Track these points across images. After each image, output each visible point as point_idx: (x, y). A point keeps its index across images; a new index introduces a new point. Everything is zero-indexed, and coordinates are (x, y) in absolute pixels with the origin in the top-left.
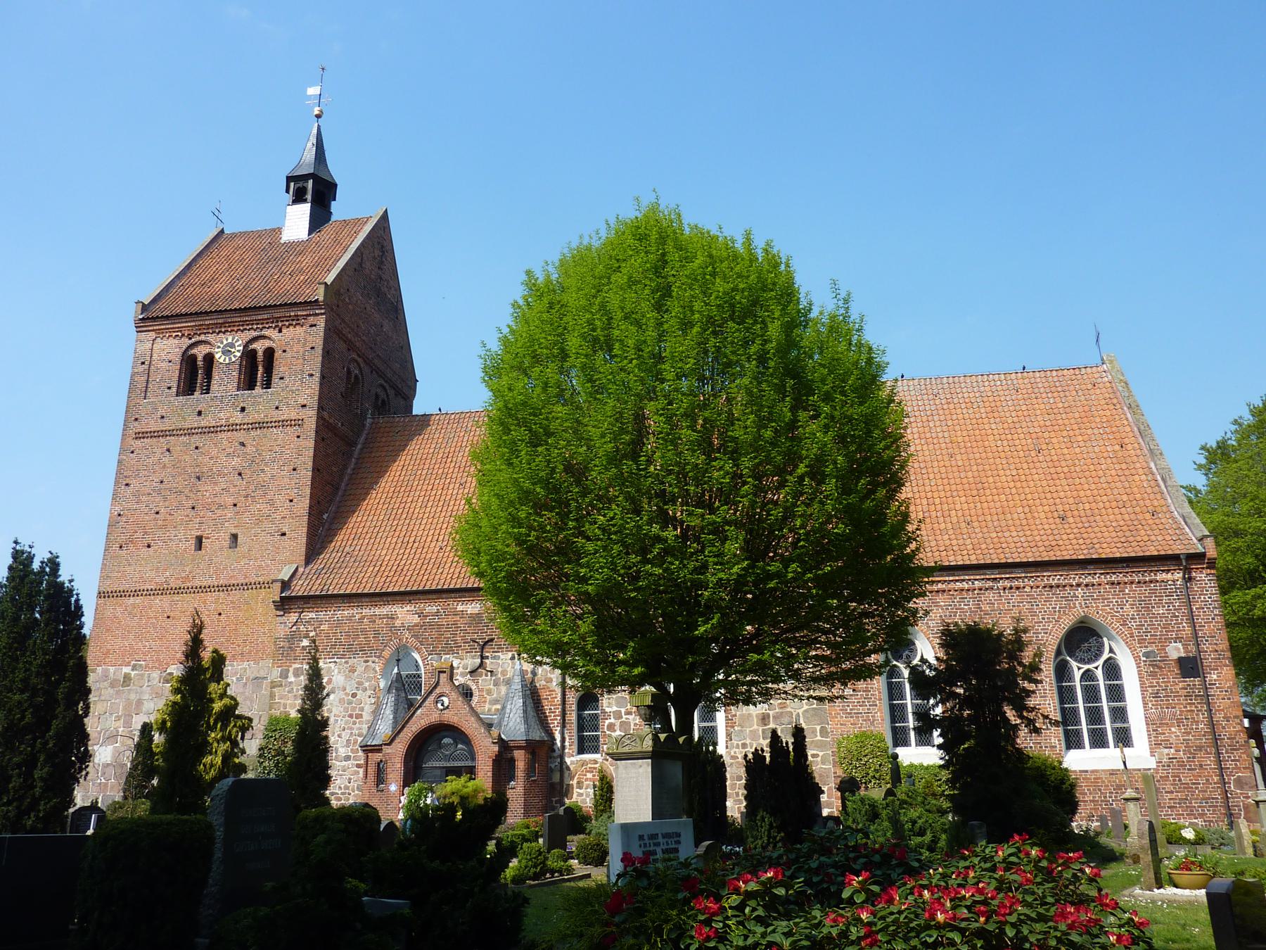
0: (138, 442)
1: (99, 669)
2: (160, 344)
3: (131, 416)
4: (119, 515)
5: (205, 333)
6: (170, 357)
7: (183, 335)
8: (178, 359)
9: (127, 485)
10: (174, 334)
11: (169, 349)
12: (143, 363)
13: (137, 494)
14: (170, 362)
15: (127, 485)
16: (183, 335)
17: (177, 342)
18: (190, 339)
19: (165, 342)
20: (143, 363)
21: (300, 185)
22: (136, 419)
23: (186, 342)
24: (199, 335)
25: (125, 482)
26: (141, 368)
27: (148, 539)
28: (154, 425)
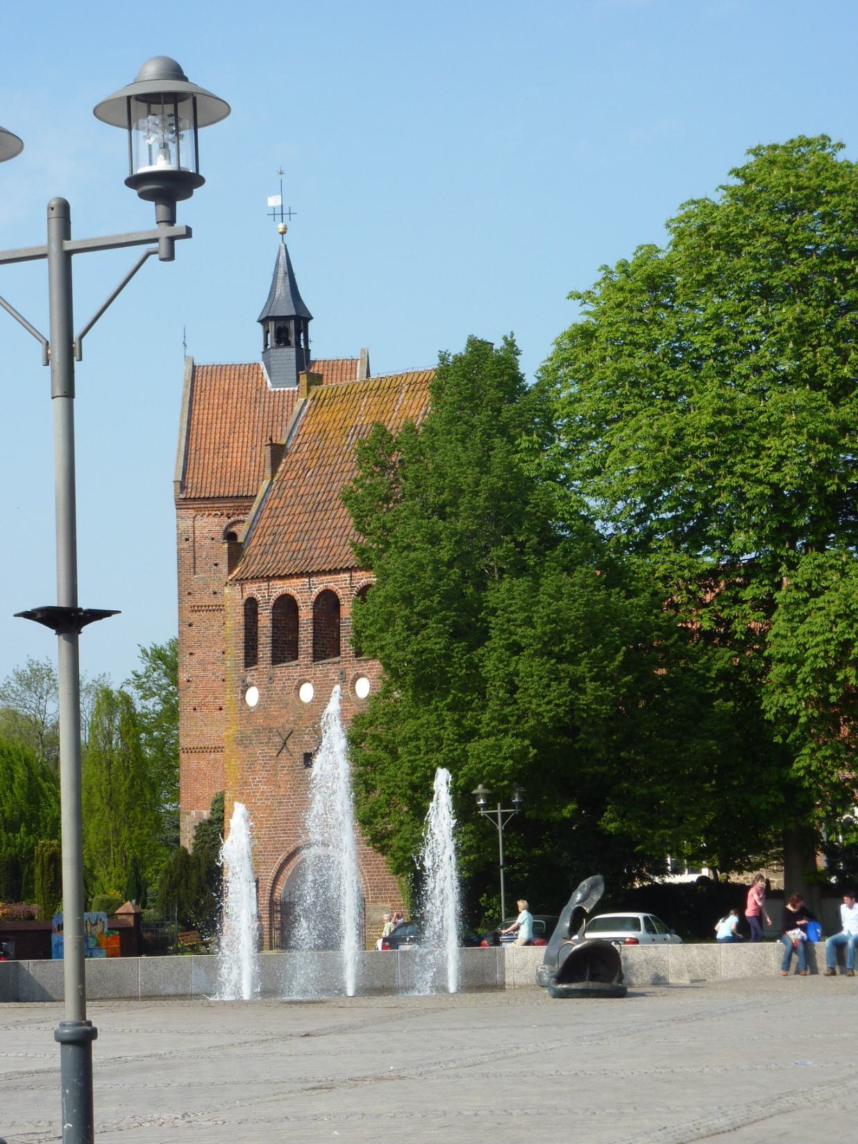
0: (195, 615)
1: (193, 813)
2: (199, 523)
3: (185, 591)
4: (189, 681)
5: (243, 514)
6: (211, 535)
7: (222, 514)
8: (220, 536)
9: (191, 654)
10: (214, 513)
11: (210, 525)
12: (187, 540)
13: (202, 663)
14: (213, 539)
15: (191, 654)
16: (222, 514)
17: (216, 520)
18: (229, 518)
19: (205, 520)
20: (187, 540)
21: (281, 324)
22: (190, 594)
23: (226, 521)
24: (238, 515)
25: (188, 652)
26: (186, 545)
27: (219, 703)
28: (207, 600)
